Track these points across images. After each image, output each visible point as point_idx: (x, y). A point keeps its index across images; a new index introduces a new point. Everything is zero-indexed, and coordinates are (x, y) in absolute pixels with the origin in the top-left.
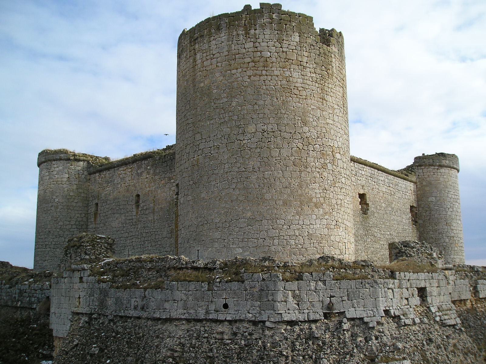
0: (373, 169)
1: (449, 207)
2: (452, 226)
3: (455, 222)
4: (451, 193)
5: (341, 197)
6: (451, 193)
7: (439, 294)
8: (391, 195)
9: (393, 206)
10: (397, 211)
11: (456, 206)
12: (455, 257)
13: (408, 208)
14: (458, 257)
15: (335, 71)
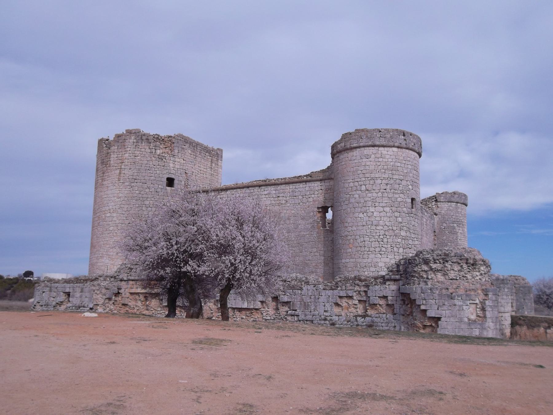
0: (253, 188)
1: (344, 199)
2: (346, 222)
3: (351, 216)
4: (348, 181)
5: (107, 239)
6: (348, 181)
7: (81, 297)
8: (280, 204)
9: (282, 215)
10: (289, 219)
11: (357, 196)
12: (348, 260)
13: (313, 212)
14: (351, 260)
15: (112, 162)
